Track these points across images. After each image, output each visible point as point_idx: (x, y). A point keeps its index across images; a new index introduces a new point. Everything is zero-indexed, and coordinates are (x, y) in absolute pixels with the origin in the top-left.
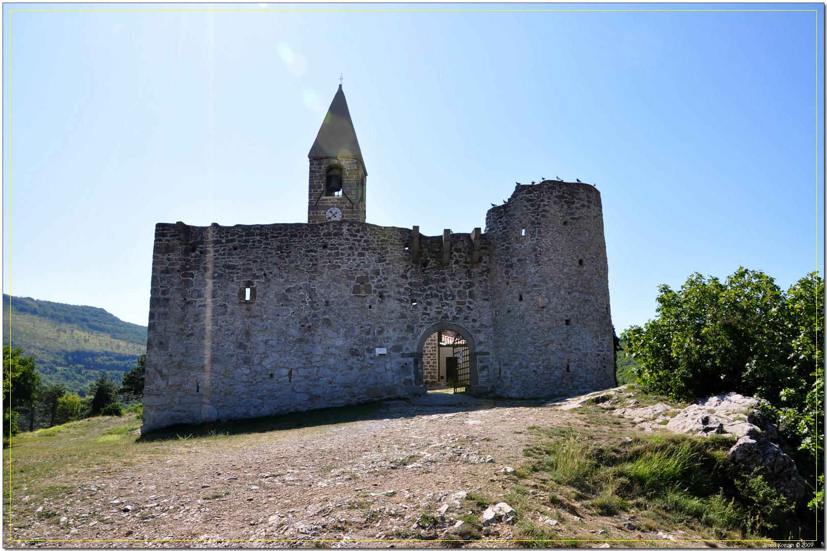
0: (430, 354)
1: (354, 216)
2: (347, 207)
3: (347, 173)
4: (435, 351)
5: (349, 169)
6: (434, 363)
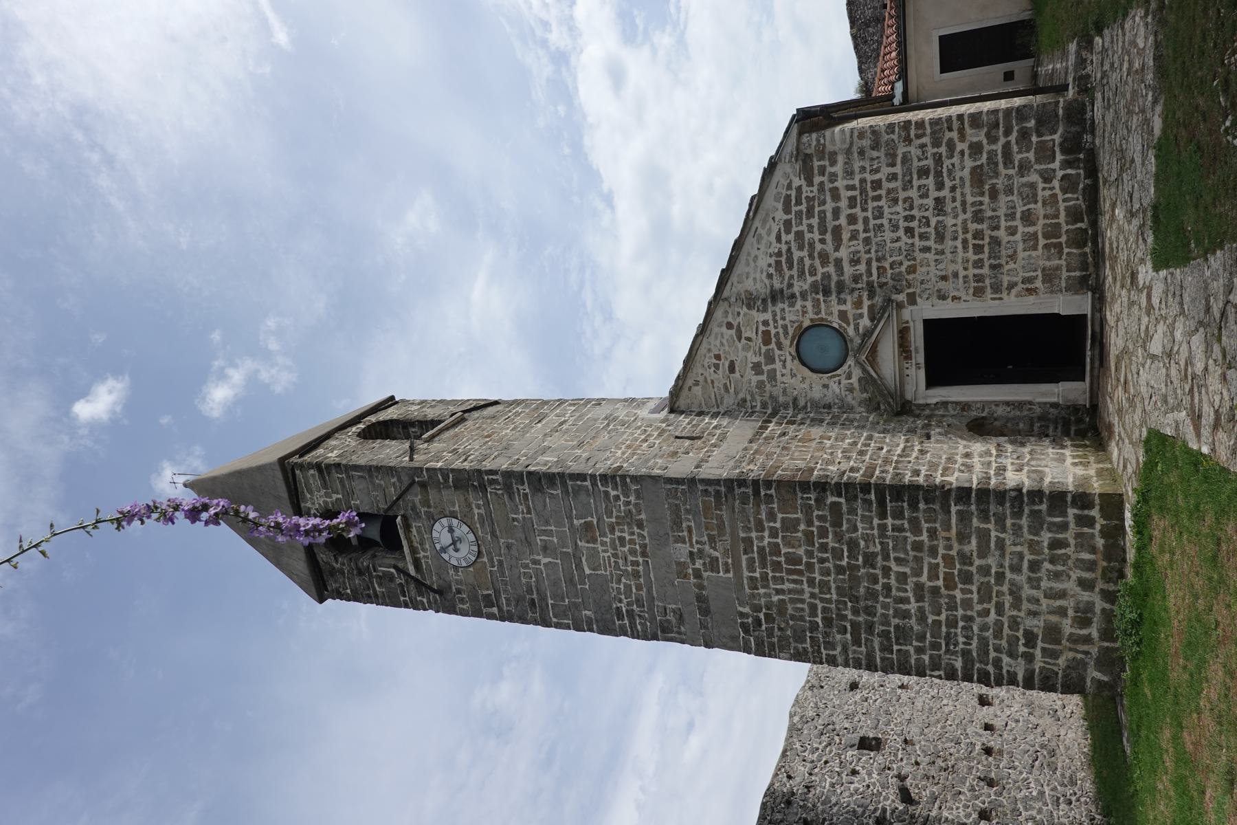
0: (936, 143)
3: (335, 496)
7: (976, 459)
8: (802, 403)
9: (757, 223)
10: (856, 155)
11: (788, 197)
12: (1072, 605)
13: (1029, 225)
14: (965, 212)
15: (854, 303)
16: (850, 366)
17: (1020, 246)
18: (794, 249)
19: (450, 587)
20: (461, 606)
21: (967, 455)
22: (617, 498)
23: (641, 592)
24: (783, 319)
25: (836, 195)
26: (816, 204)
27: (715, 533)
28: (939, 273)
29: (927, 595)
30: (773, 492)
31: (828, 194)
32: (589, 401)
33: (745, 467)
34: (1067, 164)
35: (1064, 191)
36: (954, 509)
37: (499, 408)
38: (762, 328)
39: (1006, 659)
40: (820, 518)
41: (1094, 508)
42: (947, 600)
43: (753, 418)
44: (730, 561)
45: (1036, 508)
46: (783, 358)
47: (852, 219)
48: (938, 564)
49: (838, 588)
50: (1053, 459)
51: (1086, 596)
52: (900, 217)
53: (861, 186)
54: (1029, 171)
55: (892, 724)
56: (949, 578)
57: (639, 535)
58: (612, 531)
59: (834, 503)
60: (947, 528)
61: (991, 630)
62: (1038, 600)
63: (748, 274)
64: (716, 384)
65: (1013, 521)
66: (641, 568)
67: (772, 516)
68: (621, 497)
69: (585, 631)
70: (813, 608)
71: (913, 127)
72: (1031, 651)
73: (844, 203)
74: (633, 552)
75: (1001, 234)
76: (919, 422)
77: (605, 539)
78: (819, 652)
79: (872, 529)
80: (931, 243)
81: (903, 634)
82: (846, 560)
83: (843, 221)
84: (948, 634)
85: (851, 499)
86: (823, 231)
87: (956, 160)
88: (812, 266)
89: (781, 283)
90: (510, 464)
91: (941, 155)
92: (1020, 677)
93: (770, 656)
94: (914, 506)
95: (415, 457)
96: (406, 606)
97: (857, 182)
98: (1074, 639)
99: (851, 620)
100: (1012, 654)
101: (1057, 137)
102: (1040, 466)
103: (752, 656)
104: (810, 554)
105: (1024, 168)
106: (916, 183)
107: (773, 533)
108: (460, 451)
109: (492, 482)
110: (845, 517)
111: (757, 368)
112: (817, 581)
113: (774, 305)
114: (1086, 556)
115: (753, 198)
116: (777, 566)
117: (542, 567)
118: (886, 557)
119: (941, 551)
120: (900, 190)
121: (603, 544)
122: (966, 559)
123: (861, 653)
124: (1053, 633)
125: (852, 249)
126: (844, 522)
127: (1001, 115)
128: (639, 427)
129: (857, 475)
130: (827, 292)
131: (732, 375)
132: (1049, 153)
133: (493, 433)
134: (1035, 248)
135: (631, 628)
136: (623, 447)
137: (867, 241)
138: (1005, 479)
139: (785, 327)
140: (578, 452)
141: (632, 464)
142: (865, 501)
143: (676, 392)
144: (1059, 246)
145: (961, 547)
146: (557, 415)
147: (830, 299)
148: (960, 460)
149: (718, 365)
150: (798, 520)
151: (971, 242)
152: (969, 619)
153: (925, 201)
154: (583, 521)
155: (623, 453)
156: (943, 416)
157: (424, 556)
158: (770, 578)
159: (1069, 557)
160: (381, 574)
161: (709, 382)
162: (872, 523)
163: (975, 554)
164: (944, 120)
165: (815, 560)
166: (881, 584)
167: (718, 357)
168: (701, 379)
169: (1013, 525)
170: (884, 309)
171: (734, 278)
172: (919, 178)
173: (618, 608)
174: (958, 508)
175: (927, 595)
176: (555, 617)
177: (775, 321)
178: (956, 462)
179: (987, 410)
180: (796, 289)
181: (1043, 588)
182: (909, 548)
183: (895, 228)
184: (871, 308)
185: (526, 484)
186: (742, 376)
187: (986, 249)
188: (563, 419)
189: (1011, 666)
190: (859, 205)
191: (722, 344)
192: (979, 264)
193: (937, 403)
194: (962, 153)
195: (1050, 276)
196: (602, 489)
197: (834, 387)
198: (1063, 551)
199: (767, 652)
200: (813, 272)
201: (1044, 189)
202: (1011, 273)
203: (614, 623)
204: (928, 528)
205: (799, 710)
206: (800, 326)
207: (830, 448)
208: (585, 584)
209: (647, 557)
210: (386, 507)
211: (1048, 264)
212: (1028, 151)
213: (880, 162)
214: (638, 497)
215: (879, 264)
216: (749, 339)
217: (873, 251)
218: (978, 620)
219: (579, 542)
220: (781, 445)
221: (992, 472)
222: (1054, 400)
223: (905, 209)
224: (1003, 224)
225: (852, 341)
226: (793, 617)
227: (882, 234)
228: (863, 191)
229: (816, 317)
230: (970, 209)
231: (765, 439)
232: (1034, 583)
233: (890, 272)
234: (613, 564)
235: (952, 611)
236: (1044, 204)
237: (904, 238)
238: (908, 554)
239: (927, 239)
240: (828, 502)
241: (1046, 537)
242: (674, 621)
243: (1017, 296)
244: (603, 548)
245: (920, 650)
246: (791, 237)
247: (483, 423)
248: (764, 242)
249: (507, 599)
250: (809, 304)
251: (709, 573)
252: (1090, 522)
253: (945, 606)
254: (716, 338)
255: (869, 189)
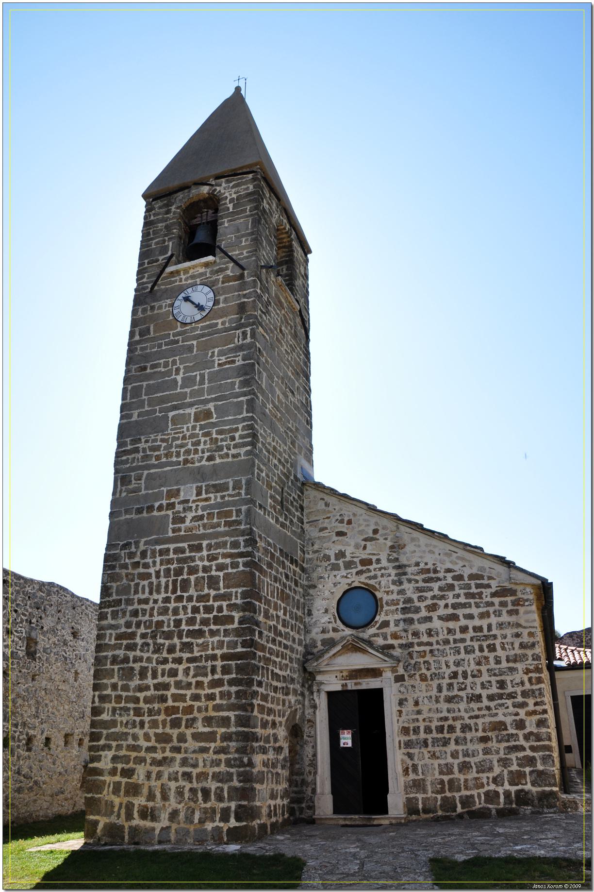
0: (525, 694)
1: (245, 296)
2: (227, 279)
3: (231, 206)
4: (539, 681)
5: (234, 196)
6: (541, 723)
7: (272, 732)
8: (311, 591)
9: (461, 553)
10: (516, 630)
11: (481, 577)
12: (157, 805)
13: (459, 768)
14: (471, 718)
15: (396, 633)
16: (343, 630)
17: (442, 762)
18: (439, 583)
19: (154, 301)
20: (140, 310)
21: (274, 724)
22: (233, 438)
23: (154, 459)
24: (382, 576)
25: (484, 615)
26: (477, 600)
27: (205, 521)
28: (420, 700)
29: (160, 693)
30: (241, 568)
31: (485, 610)
32: (310, 415)
33: (261, 544)
34: (507, 794)
35: (487, 794)
36: (231, 714)
37: (303, 342)
38: (374, 558)
39: (110, 754)
40: (220, 609)
41: (237, 821)
42: (156, 708)
43: (299, 552)
44: (182, 533)
45: (235, 778)
46: (349, 576)
47: (464, 629)
48: (186, 702)
49: (163, 622)
50: (273, 789)
51: (164, 816)
52: (466, 668)
53: (491, 636)
54: (503, 766)
55: (48, 665)
56: (175, 710)
57: (202, 457)
58: (205, 435)
59: (233, 618)
60: (217, 708)
61: (134, 743)
62: (159, 780)
63: (419, 546)
64: (326, 520)
65: (223, 760)
66: (174, 459)
67: (220, 568)
68: (234, 442)
69: (121, 412)
70: (146, 601)
71: (538, 675)
72: (119, 774)
73: (477, 622)
74: (188, 452)
75: (452, 747)
76: (298, 687)
77: (198, 429)
78: (109, 606)
79: (213, 649)
80: (445, 692)
81: (128, 674)
82: (186, 628)
83: (463, 622)
84: (128, 709)
85: (238, 632)
86: (455, 606)
87: (511, 709)
88: (426, 598)
89: (412, 574)
90: (259, 349)
91: (516, 697)
92: (95, 765)
93: (105, 566)
94: (231, 683)
95: (264, 270)
96: (140, 265)
97: (494, 632)
98: (129, 807)
99: (137, 632)
100: (115, 759)
101: (528, 787)
102: (268, 780)
103: (104, 552)
104: (190, 599)
105: (504, 762)
106: (493, 679)
107: (206, 569)
108: (269, 308)
109: (244, 334)
110: (222, 628)
111: (341, 555)
112: (168, 605)
113: (394, 568)
114: (197, 816)
115: (482, 549)
116: (179, 572)
117: (173, 377)
118: (190, 660)
119: (196, 704)
120: (488, 667)
121: (194, 428)
122: (191, 723)
123: (110, 640)
124: (134, 790)
125: (440, 631)
126: (218, 627)
127: (547, 743)
128: (290, 457)
129: (257, 636)
130: (404, 610)
131: (334, 534)
132: (516, 781)
133: (283, 335)
134: (441, 773)
135: (124, 451)
136: (274, 444)
137: (446, 642)
138: (257, 753)
139: (375, 577)
140: (270, 406)
141: (261, 451)
142: (236, 643)
143: (319, 486)
144: (442, 791)
145: (200, 720)
146: (298, 388)
147: (399, 613)
148: (270, 718)
149: (343, 523)
150: (219, 589)
151: (446, 724)
152: (142, 725)
153: (479, 686)
154: (213, 410)
155: (270, 444)
156: (304, 705)
157: (181, 279)
158: (169, 566)
159: (195, 802)
160: (166, 243)
161: (328, 515)
162: (218, 649)
163: (195, 731)
164: (543, 699)
165: (185, 603)
166: (167, 656)
167: (349, 522)
168: (331, 508)
169: (220, 760)
170: (391, 656)
171: (416, 534)
172: (498, 682)
173: (140, 439)
174: (233, 719)
175: (160, 693)
176: (132, 388)
177: (380, 569)
178: (268, 715)
179: (309, 739)
180: (406, 586)
181: (169, 783)
182: (199, 679)
183: (457, 664)
184: (392, 647)
185: (243, 363)
186: (333, 542)
187: (440, 736)
188: (296, 393)
189: (105, 757)
190: (475, 634)
191: (359, 525)
192: (428, 730)
193: (314, 700)
194: (517, 714)
195: (419, 785)
196: (240, 426)
197: (325, 619)
198: (200, 798)
199: (108, 564)
200: (421, 599)
201: (488, 778)
202: (421, 755)
203: (127, 438)
204: (215, 693)
205: (56, 589)
206: (376, 590)
207: (276, 614)
208: (160, 412)
209: (184, 464)
210: (222, 247)
211: (428, 783)
212: (518, 765)
213: (509, 649)
214: (234, 456)
215: (428, 652)
216: (365, 548)
217: (438, 646)
218: (141, 733)
219: (196, 406)
220: (279, 576)
221: (262, 744)
222: (318, 790)
223: (472, 672)
224: (460, 748)
225: (364, 632)
226: (137, 585)
227: (452, 654)
228: (487, 637)
229: (384, 602)
230: (472, 722)
231: (283, 562)
232: (174, 777)
233: (421, 660)
234: (177, 436)
235: (148, 712)
236: (476, 779)
237: (448, 672)
238: (193, 677)
239: (448, 690)
240: (234, 614)
241: (213, 785)
242: (130, 487)
243: (403, 761)
244: (190, 428)
245: (114, 687)
246: (450, 581)
247: (291, 327)
248: (446, 558)
249: (146, 348)
250: (395, 596)
251: (171, 517)
252: (225, 818)
253: (151, 707)
254: (365, 520)
255: (488, 642)
